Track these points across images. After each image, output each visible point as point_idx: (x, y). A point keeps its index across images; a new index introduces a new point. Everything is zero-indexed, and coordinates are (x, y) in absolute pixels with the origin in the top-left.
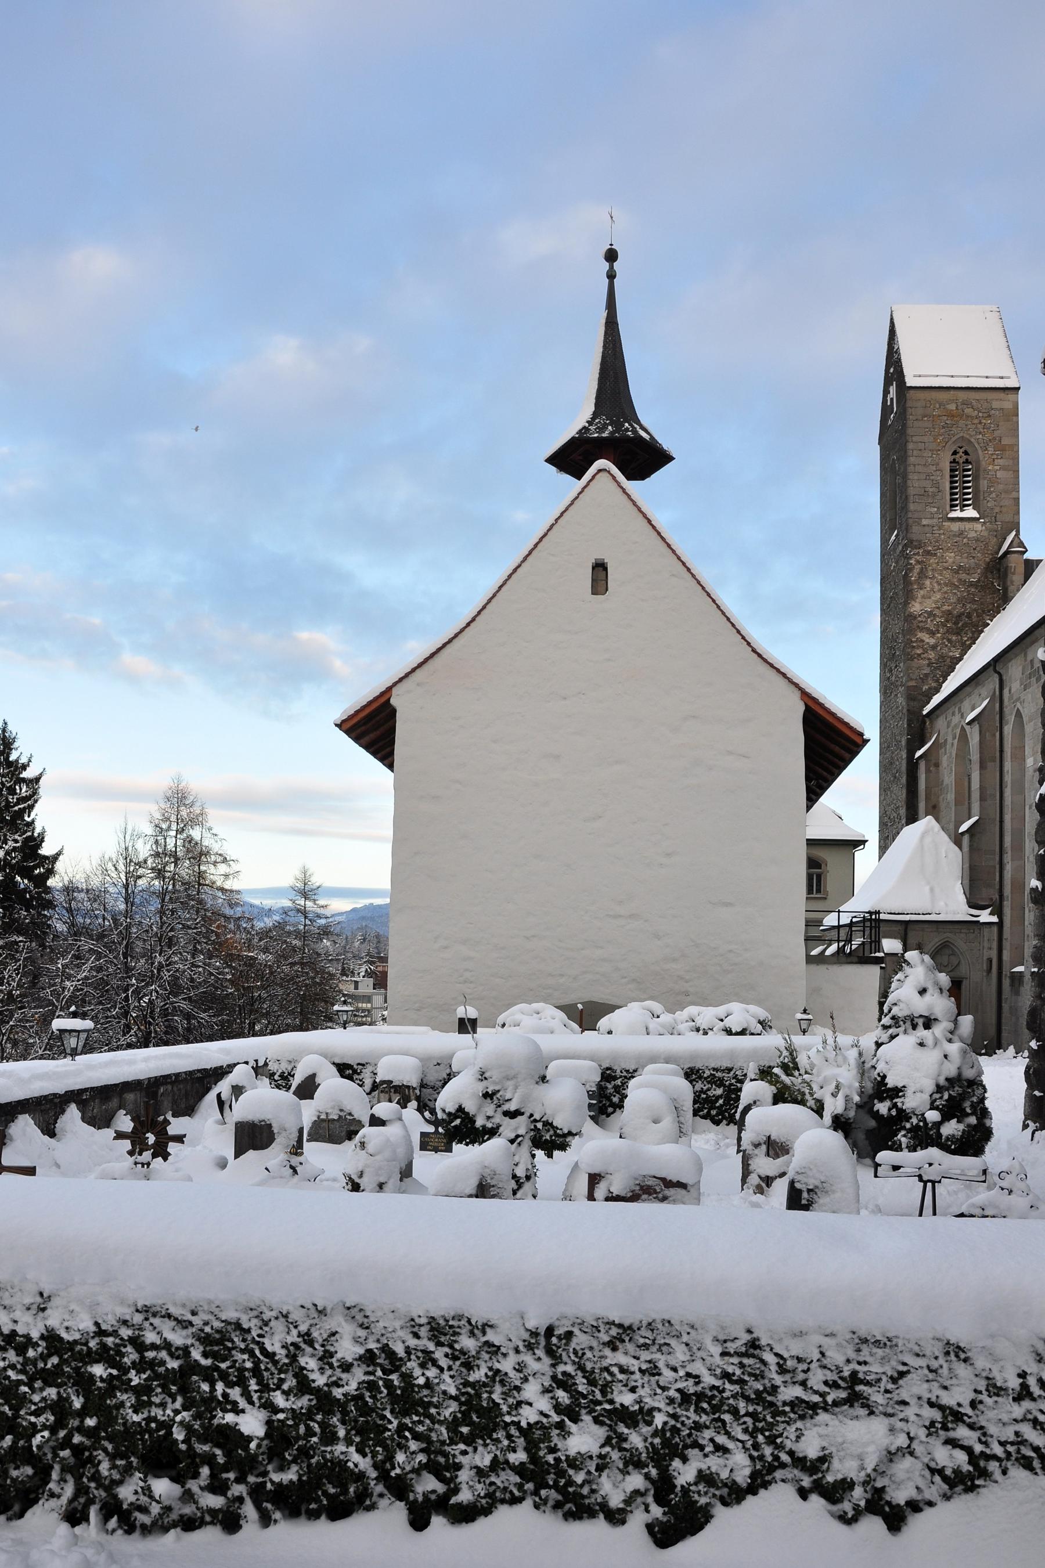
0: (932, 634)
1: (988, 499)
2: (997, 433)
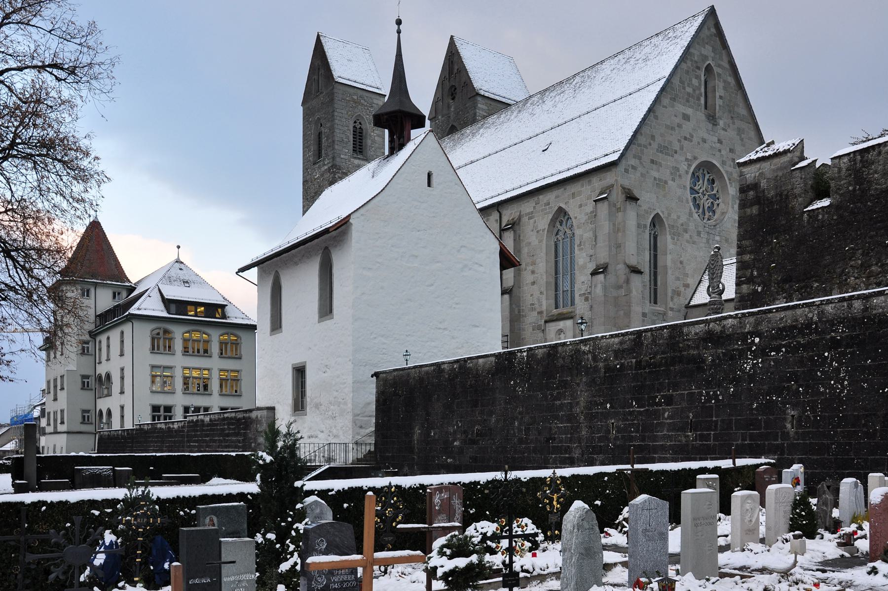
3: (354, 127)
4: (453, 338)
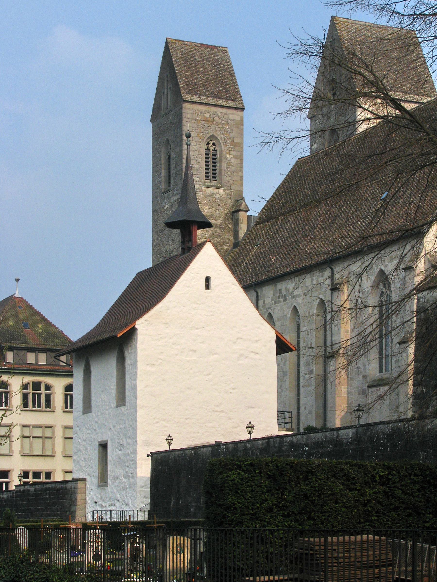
1: (227, 175)
2: (232, 135)
3: (207, 149)
4: (230, 419)
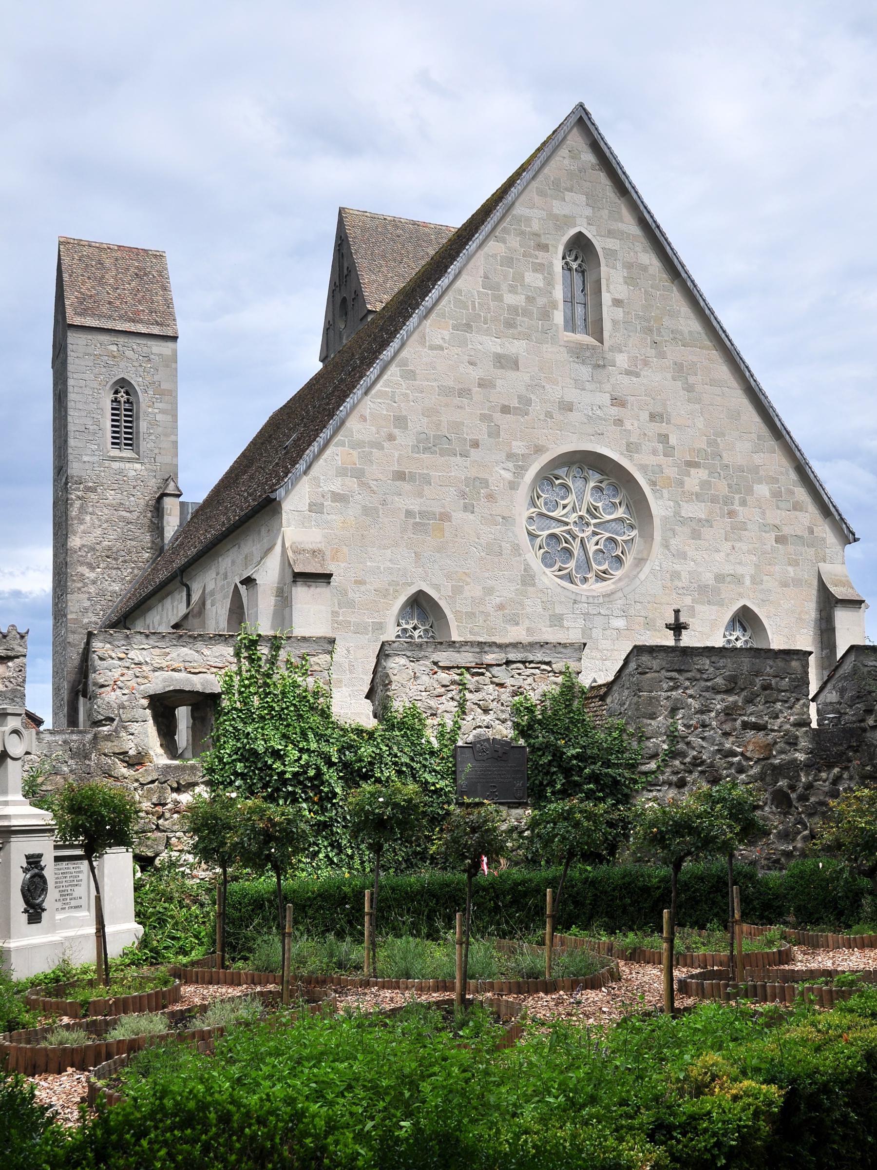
0: (92, 568)
